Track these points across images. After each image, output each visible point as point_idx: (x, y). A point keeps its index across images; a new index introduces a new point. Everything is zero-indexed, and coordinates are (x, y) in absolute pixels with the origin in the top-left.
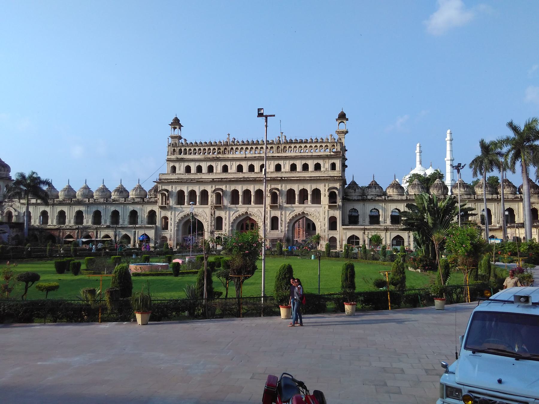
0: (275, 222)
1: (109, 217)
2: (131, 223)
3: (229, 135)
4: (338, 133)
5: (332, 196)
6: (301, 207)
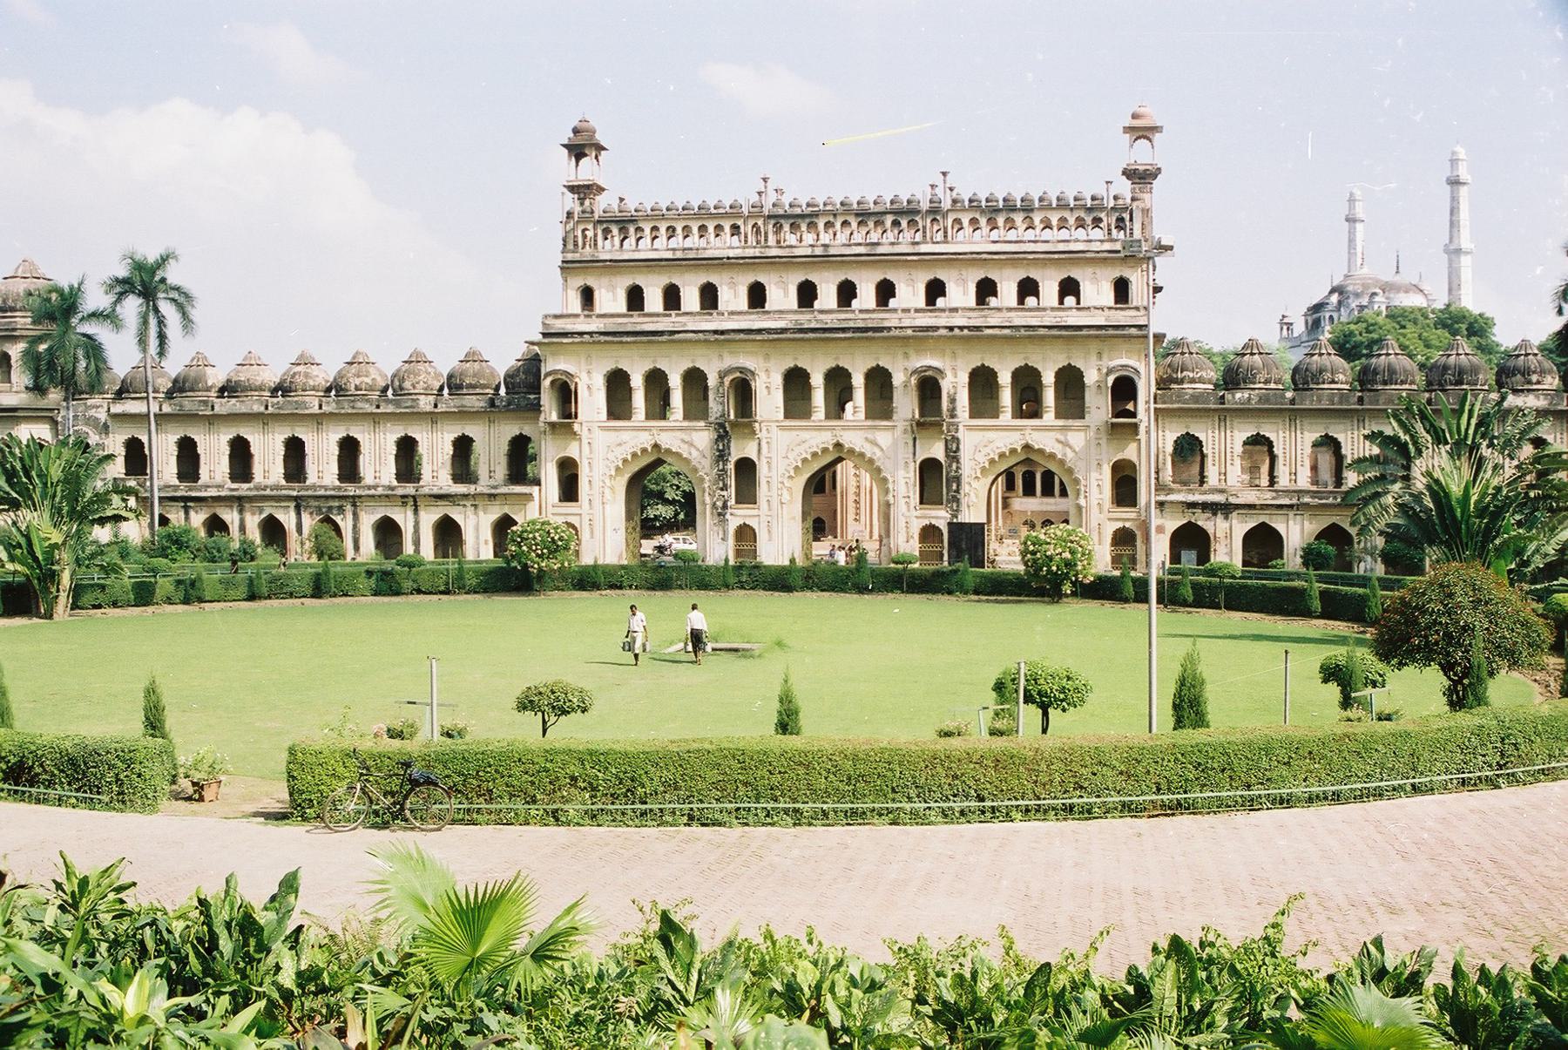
4: (1129, 174)
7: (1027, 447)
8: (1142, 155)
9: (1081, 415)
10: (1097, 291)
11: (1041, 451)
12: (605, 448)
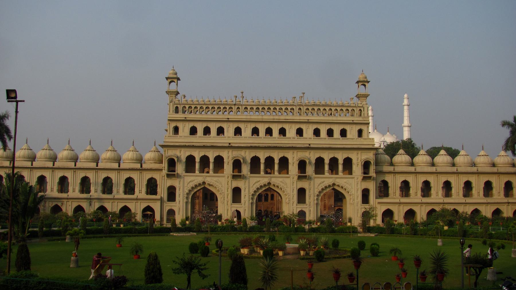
1: (56, 184)
2: (125, 193)
3: (242, 93)
5: (366, 165)
6: (332, 178)
8: (362, 90)
10: (352, 132)
11: (338, 186)
12: (186, 183)
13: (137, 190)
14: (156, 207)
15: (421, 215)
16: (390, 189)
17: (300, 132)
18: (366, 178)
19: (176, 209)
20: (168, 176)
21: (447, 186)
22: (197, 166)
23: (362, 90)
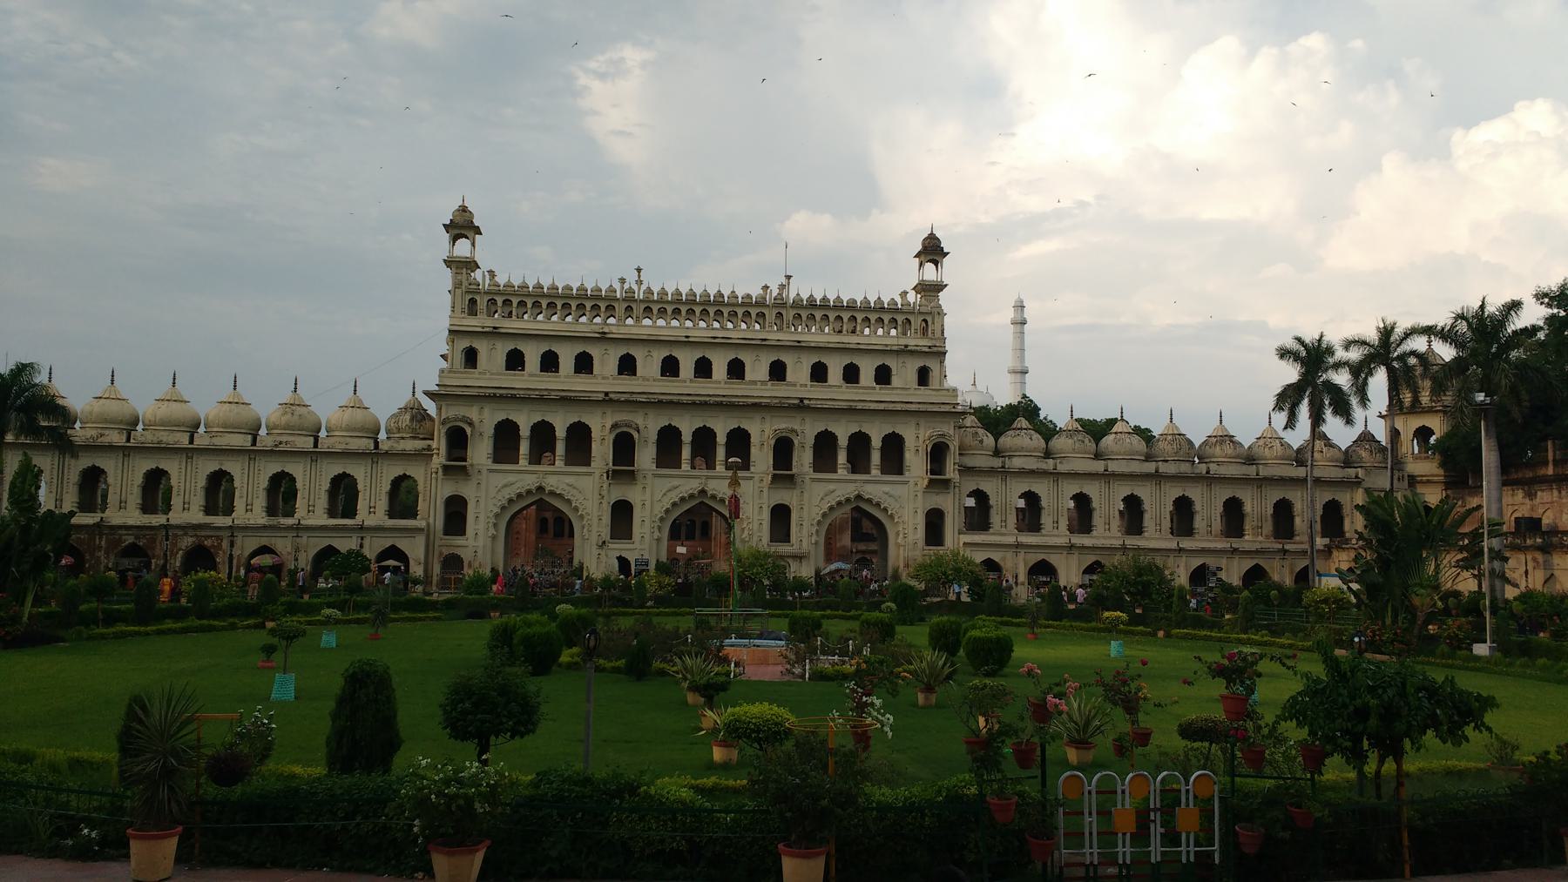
0: (781, 515)
3: (639, 270)
5: (938, 453)
6: (855, 481)
7: (859, 497)
8: (930, 273)
9: (900, 472)
10: (905, 374)
11: (869, 501)
12: (493, 489)
13: (362, 505)
14: (415, 549)
15: (1070, 574)
16: (993, 512)
17: (778, 372)
18: (938, 483)
19: (466, 555)
20: (447, 469)
21: (1133, 507)
22: (524, 448)
23: (930, 273)
